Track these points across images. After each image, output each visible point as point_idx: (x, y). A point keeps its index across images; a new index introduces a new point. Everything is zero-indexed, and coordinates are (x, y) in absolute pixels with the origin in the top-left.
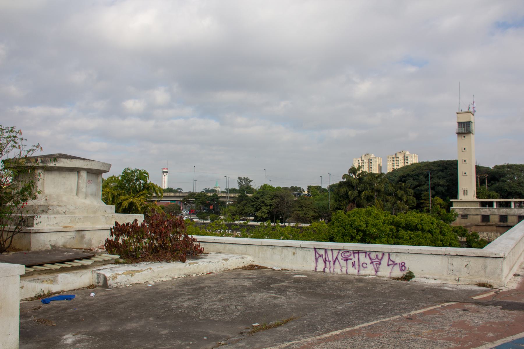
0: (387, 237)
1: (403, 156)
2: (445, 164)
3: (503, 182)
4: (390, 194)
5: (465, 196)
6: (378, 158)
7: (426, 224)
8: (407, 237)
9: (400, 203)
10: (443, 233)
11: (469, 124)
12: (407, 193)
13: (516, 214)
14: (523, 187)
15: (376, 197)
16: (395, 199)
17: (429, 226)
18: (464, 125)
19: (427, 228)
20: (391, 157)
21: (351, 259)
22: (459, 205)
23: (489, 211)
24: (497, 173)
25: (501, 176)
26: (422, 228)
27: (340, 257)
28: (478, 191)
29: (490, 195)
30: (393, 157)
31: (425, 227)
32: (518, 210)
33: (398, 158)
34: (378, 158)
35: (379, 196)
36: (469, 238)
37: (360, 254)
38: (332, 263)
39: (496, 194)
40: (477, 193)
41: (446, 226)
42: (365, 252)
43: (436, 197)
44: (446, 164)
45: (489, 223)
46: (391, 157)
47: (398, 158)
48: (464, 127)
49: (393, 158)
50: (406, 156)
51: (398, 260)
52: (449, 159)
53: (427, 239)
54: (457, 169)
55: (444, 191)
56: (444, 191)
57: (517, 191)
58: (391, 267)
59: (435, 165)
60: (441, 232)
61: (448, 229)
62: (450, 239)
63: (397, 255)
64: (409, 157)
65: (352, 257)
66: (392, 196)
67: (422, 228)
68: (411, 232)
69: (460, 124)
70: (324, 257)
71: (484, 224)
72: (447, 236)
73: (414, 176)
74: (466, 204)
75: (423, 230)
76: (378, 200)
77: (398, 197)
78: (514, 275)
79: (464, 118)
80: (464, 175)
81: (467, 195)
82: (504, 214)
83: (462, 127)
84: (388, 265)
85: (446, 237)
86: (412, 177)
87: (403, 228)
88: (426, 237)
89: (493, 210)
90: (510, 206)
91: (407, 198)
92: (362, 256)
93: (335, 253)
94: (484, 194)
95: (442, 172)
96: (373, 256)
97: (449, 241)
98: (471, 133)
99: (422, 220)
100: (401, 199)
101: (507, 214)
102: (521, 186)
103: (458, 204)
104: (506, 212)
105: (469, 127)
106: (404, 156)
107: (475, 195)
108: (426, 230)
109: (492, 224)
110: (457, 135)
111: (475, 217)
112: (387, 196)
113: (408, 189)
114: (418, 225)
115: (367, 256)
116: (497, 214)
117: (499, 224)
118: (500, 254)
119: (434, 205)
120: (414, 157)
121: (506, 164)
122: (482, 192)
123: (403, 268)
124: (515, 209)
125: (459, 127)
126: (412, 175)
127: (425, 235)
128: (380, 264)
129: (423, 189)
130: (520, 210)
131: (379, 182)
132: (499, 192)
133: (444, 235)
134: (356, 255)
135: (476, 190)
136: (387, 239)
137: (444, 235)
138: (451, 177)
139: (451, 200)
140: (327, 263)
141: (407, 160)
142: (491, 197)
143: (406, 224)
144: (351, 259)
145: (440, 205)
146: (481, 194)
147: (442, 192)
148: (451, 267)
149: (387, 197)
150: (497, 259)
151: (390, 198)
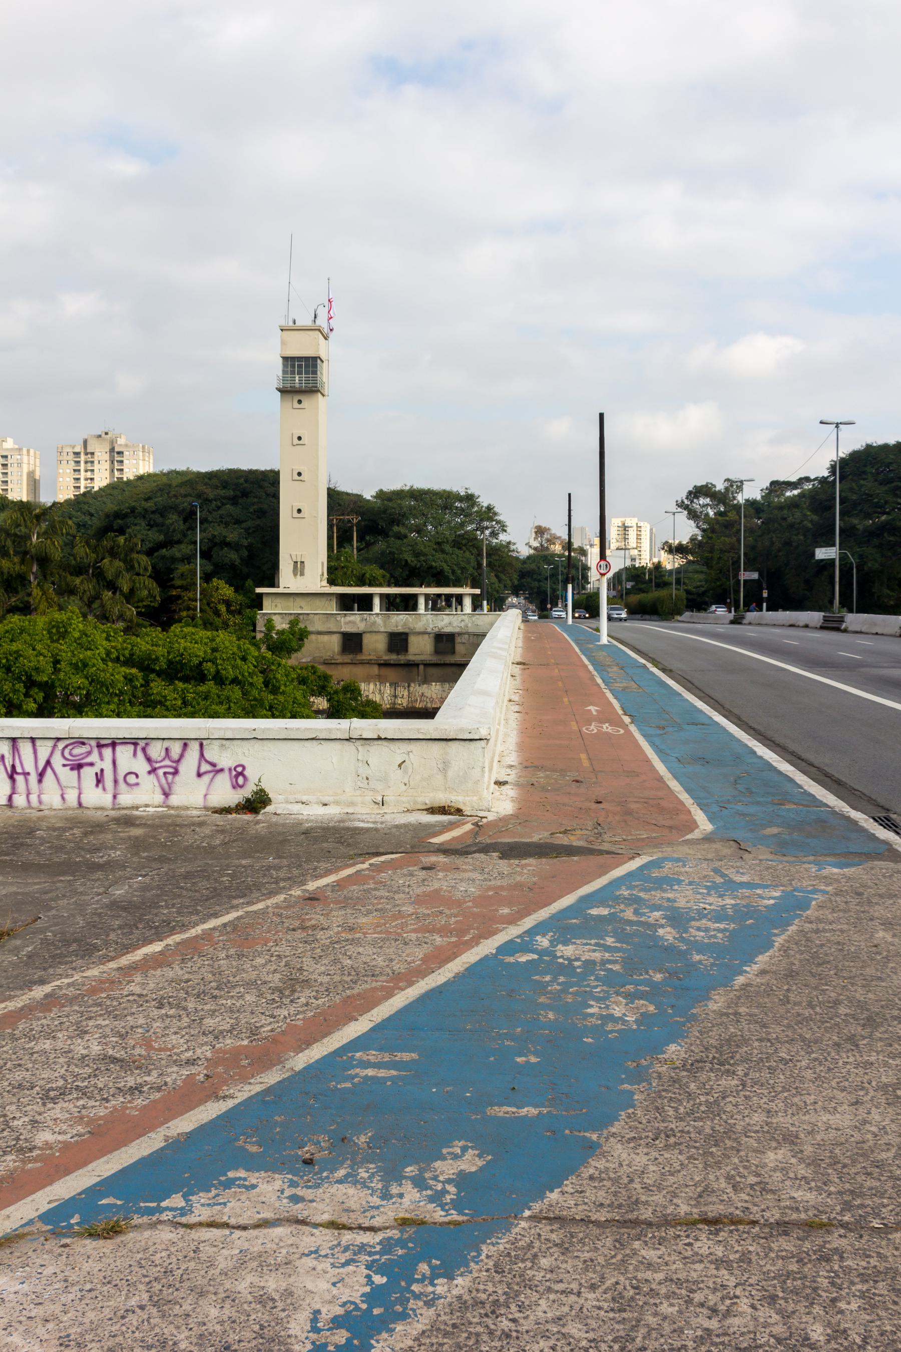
0: (116, 700)
1: (108, 450)
2: (242, 481)
3: (399, 538)
4: (79, 570)
5: (298, 576)
6: (28, 451)
7: (228, 659)
8: (175, 699)
9: (112, 599)
10: (274, 686)
11: (315, 366)
12: (132, 567)
13: (429, 630)
14: (447, 554)
15: (35, 578)
16: (97, 586)
17: (234, 667)
18: (300, 366)
19: (231, 673)
20: (70, 450)
21: (91, 764)
22: (279, 605)
23: (362, 620)
24: (385, 512)
25: (393, 522)
26: (218, 672)
27: (57, 761)
29: (364, 575)
30: (77, 450)
31: (225, 669)
32: (434, 618)
33: (93, 454)
34: (28, 451)
35: (44, 575)
36: (336, 699)
37: (119, 749)
38: (33, 778)
39: (379, 572)
40: (329, 568)
41: (279, 665)
42: (134, 742)
43: (215, 581)
44: (246, 481)
45: (360, 657)
47: (93, 454)
48: (300, 373)
49: (77, 454)
50: (117, 450)
51: (226, 759)
52: (254, 468)
53: (232, 705)
54: (276, 496)
55: (237, 563)
57: (433, 564)
58: (206, 778)
59: (215, 481)
60: (266, 684)
61: (287, 676)
62: (294, 702)
63: (222, 745)
64: (126, 453)
65: (94, 757)
66: (85, 576)
67: (218, 672)
68: (186, 685)
69: (289, 361)
70: (8, 762)
71: (347, 658)
72: (283, 693)
73: (152, 516)
74: (300, 601)
75: (219, 679)
76: (42, 589)
77: (105, 578)
78: (496, 783)
79: (301, 347)
80: (296, 514)
81: (302, 574)
82: (400, 629)
83: (293, 373)
84: (199, 775)
85: (281, 698)
86: (144, 517)
87: (159, 674)
88: (228, 699)
89: (372, 617)
90: (415, 608)
91: (134, 581)
92: (124, 753)
93: (44, 750)
94: (349, 572)
95: (233, 504)
96: (156, 751)
97: (290, 707)
98: (318, 391)
99: (214, 650)
100: (112, 586)
101: (406, 631)
102: (443, 551)
103: (278, 601)
104: (405, 624)
105: (315, 373)
106: (112, 450)
107: (326, 576)
108: (227, 678)
109: (368, 658)
110: (279, 393)
111: (326, 638)
112: (71, 574)
113: (135, 556)
114: (204, 664)
115: (140, 753)
116: (382, 630)
117: (386, 657)
118: (481, 730)
119: (208, 604)
120: (141, 454)
121: (407, 488)
122: (343, 567)
123: (241, 780)
124: (429, 616)
125: (284, 372)
126: (146, 510)
127: (225, 693)
128: (176, 772)
129: (178, 555)
130: (440, 617)
131: (45, 533)
132: (387, 566)
133: (275, 691)
134: (107, 752)
135: (328, 562)
136: (118, 708)
137: (275, 691)
138: (258, 522)
139: (259, 590)
140: (20, 779)
141: (122, 462)
142: (367, 581)
143: (170, 663)
144: (91, 764)
145: (228, 603)
146: (340, 573)
147: (233, 566)
148: (364, 771)
149: (69, 578)
150: (473, 744)
151: (82, 582)
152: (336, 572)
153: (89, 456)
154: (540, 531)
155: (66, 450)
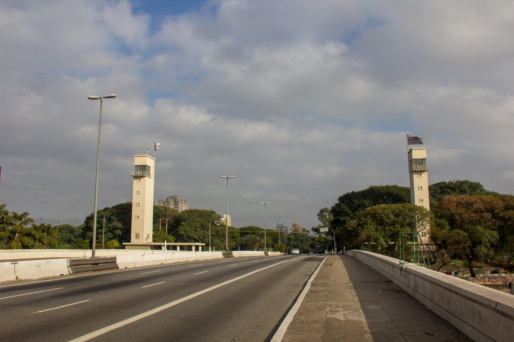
1: (174, 201)
11: (145, 168)
18: (140, 168)
20: (163, 201)
28: (154, 235)
30: (164, 201)
33: (169, 202)
40: (153, 236)
46: (163, 201)
47: (169, 202)
48: (140, 170)
49: (165, 203)
50: (176, 201)
55: (121, 234)
56: (121, 234)
64: (179, 202)
80: (137, 218)
81: (138, 238)
83: (138, 170)
106: (175, 201)
110: (133, 177)
120: (184, 202)
139: (124, 244)
141: (178, 205)
146: (157, 238)
152: (156, 237)
153: (168, 203)
154: (294, 226)
155: (161, 201)
